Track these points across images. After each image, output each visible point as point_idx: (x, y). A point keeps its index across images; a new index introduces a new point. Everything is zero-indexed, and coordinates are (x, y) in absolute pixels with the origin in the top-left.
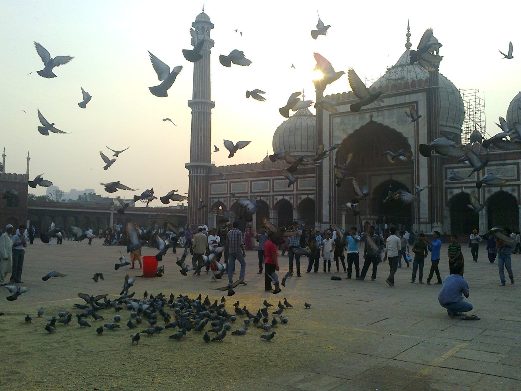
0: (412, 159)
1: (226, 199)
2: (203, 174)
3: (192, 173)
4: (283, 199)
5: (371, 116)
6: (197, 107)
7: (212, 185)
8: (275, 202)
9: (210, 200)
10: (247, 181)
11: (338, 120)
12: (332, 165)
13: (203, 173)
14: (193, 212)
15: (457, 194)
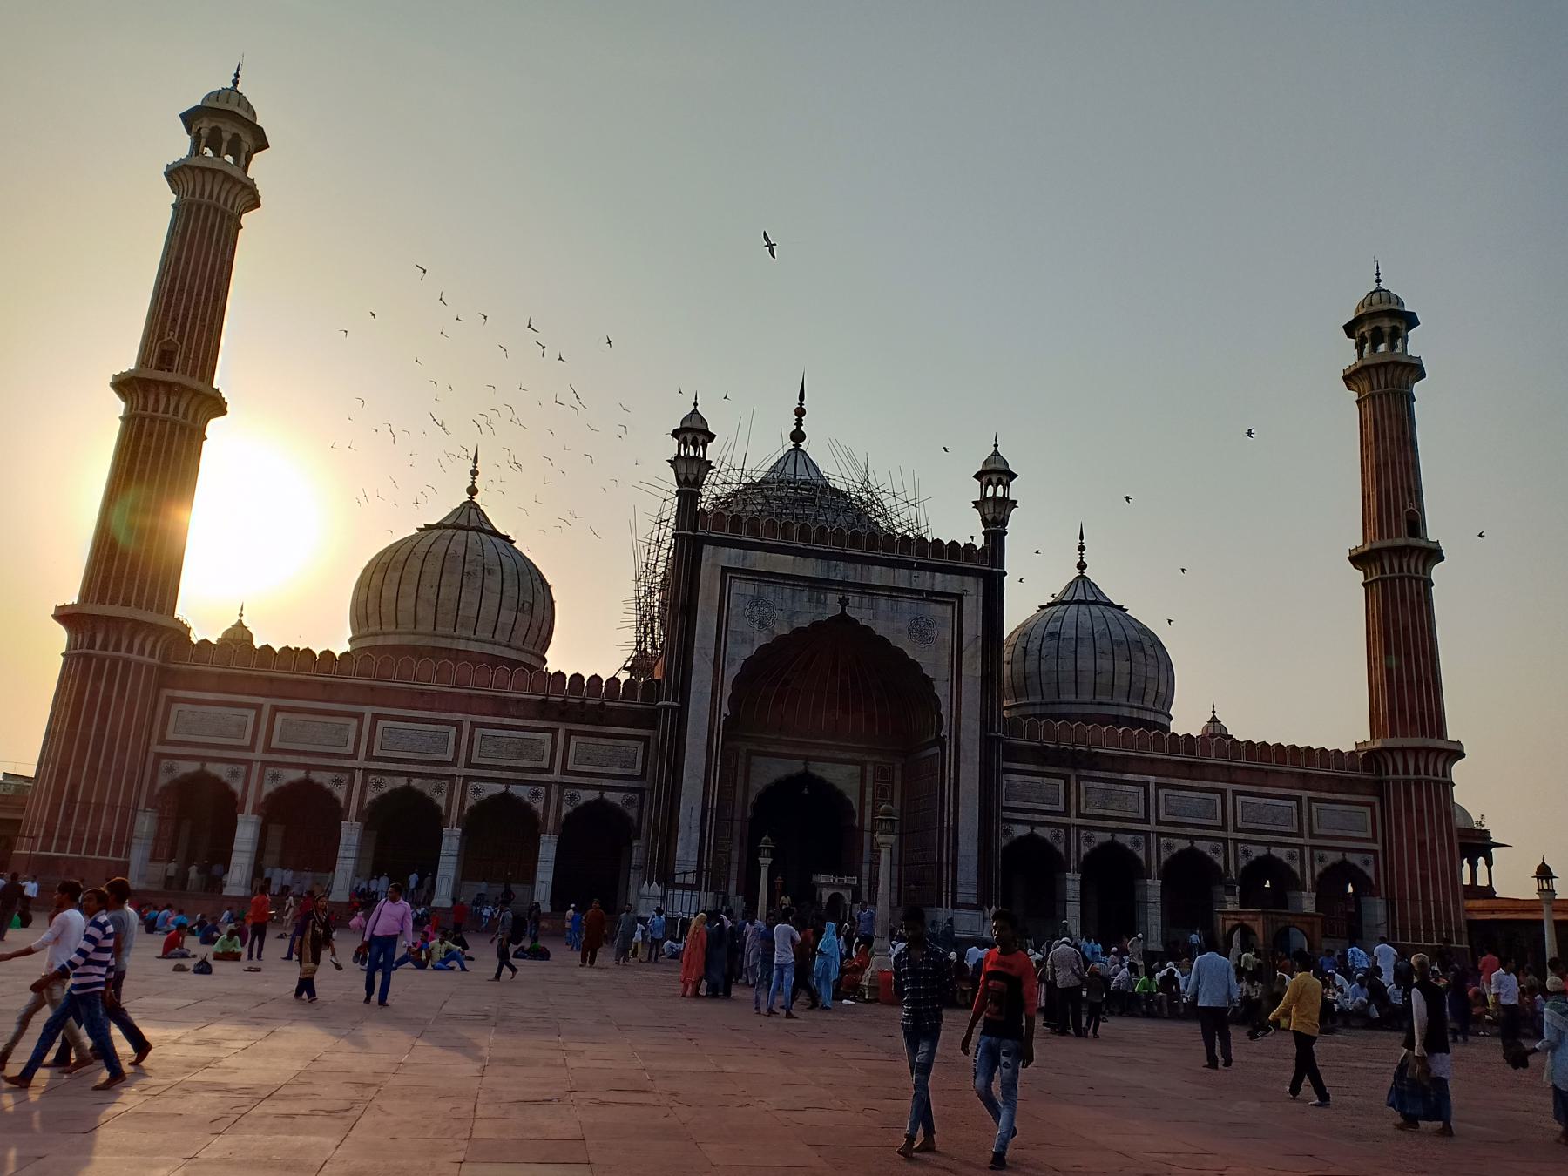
0: (942, 735)
1: (243, 768)
2: (151, 660)
3: (104, 647)
4: (505, 797)
5: (844, 602)
6: (168, 400)
7: (176, 708)
8: (471, 801)
9: (156, 764)
10: (360, 716)
11: (749, 588)
12: (720, 718)
13: (152, 655)
14: (86, 802)
15: (1020, 838)
